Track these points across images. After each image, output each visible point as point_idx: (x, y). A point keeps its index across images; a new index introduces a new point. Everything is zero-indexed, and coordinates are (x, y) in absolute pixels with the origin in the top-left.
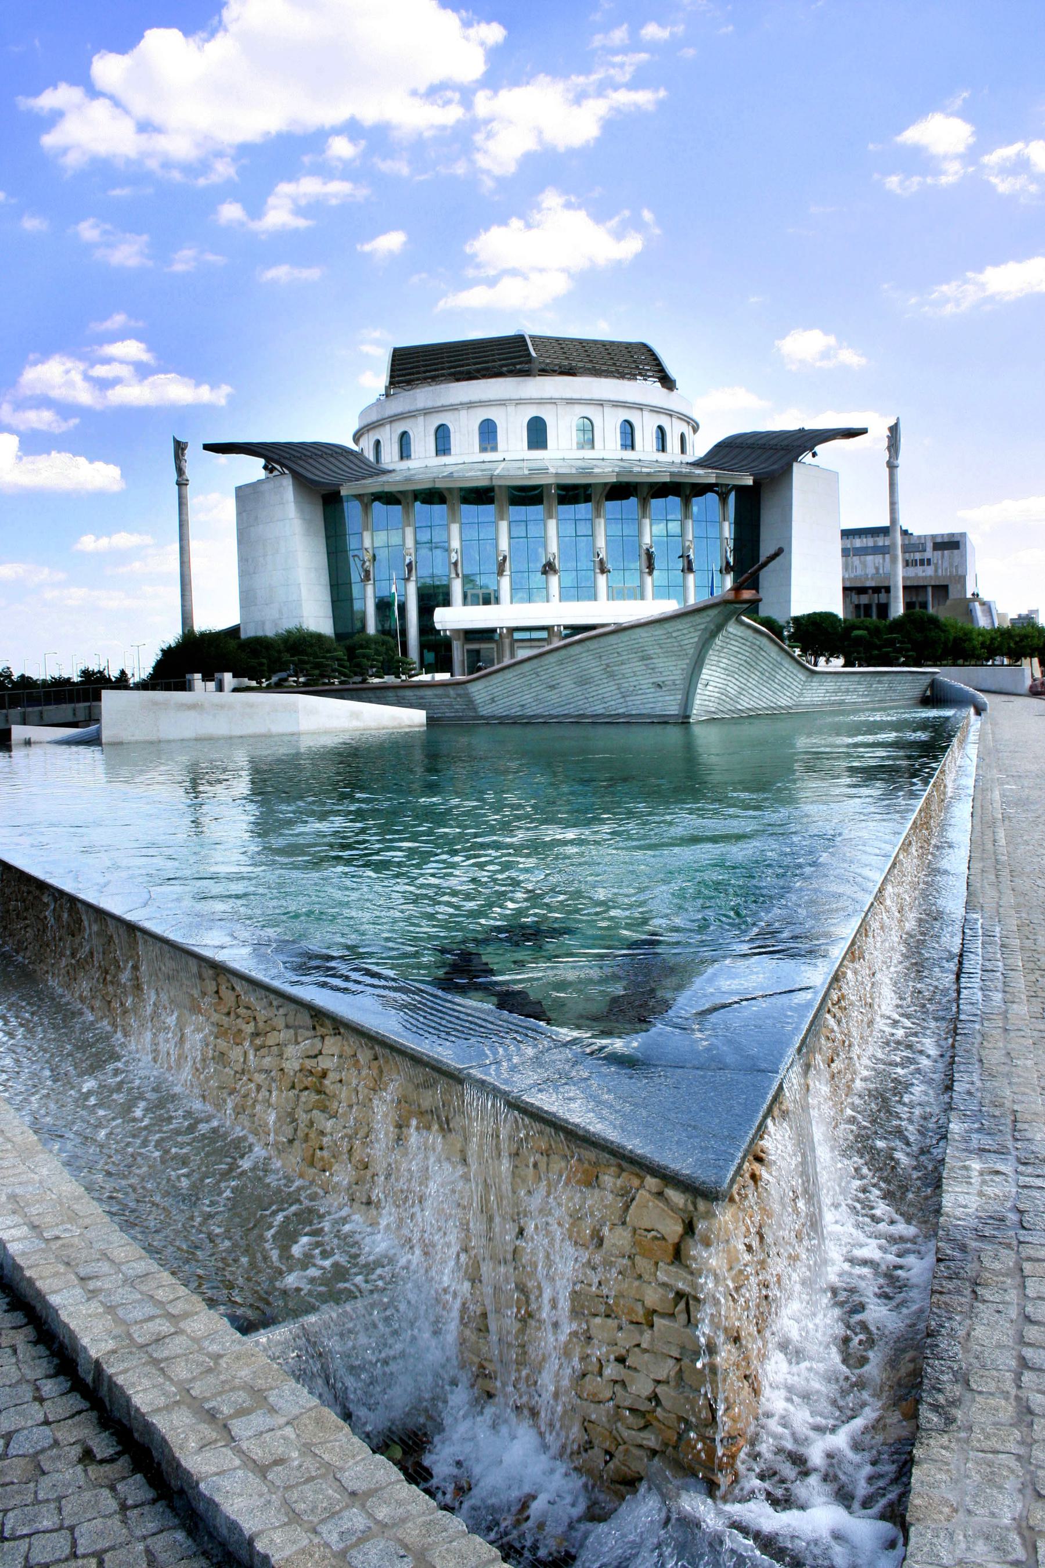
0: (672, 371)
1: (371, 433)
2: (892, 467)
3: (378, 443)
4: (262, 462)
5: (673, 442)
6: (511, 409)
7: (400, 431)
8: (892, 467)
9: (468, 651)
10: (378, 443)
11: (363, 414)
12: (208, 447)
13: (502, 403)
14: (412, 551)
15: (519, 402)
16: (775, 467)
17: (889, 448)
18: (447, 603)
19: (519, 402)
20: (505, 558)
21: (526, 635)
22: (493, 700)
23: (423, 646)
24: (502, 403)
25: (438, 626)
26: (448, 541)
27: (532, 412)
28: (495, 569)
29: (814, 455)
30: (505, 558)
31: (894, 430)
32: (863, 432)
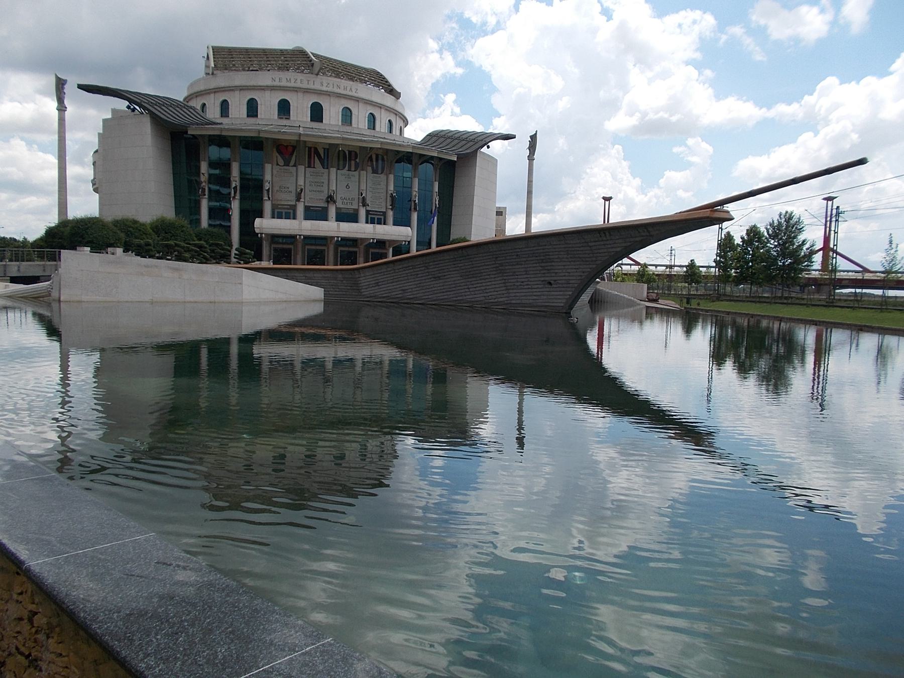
0: (397, 87)
1: (199, 99)
2: (531, 158)
3: (204, 105)
4: (127, 103)
5: (396, 131)
6: (300, 95)
7: (224, 98)
8: (531, 158)
9: (275, 250)
10: (204, 105)
11: (191, 85)
12: (81, 87)
13: (295, 90)
14: (238, 179)
15: (307, 91)
16: (468, 151)
17: (529, 148)
18: (261, 215)
19: (307, 91)
20: (302, 190)
21: (313, 242)
22: (377, 284)
23: (242, 243)
24: (295, 90)
25: (257, 231)
26: (263, 175)
27: (315, 99)
28: (294, 198)
29: (488, 147)
30: (302, 190)
31: (534, 138)
32: (513, 137)
